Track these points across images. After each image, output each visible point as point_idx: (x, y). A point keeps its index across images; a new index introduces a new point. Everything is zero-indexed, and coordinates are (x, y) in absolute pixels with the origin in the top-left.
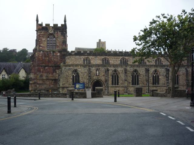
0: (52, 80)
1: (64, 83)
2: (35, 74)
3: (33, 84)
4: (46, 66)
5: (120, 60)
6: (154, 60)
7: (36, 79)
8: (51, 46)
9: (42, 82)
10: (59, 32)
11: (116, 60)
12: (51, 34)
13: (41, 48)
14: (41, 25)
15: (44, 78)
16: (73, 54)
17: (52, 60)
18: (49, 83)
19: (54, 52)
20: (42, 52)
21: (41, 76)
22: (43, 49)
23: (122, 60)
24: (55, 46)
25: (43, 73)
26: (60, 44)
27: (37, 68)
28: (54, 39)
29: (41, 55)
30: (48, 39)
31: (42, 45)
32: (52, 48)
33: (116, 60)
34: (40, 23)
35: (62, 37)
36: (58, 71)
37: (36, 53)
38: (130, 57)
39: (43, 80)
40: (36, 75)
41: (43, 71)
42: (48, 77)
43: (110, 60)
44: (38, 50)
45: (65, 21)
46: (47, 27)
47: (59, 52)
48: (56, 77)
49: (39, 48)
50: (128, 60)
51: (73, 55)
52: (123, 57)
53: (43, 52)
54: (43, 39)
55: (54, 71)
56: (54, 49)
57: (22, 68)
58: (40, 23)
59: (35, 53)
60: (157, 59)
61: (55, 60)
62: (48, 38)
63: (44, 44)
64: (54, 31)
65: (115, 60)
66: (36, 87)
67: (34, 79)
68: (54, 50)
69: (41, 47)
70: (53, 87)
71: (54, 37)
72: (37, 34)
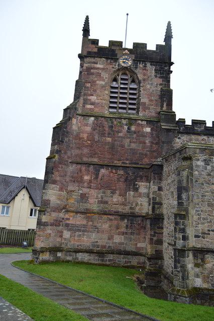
0: (123, 216)
1: (200, 227)
2: (61, 189)
3: (52, 225)
4: (102, 166)
7: (65, 209)
8: (120, 106)
9: (84, 222)
10: (148, 65)
12: (124, 70)
13: (89, 106)
14: (95, 42)
15: (95, 207)
16: (199, 130)
17: (123, 146)
18: (110, 226)
19: (131, 121)
20: (92, 119)
21: (84, 197)
22: (96, 110)
24: (135, 107)
25: (90, 187)
26: (151, 100)
27: (72, 168)
28: (131, 87)
29: (89, 129)
30: (114, 84)
31: (93, 98)
32: (125, 111)
34: (92, 36)
35: (160, 81)
36: (143, 187)
37: (74, 121)
39: (86, 213)
40: (64, 193)
41: (90, 181)
42: (106, 202)
44: (80, 111)
45: (168, 37)
46: (113, 48)
47: (149, 122)
48: (137, 204)
49: (84, 106)
51: (199, 134)
53: (96, 117)
54: (98, 82)
55: (131, 184)
56: (133, 114)
57: (24, 187)
58: (92, 36)
59: (70, 119)
61: (133, 146)
62: (114, 83)
63: (100, 100)
64: (136, 61)
66: (59, 239)
67: (58, 209)
68: (131, 116)
69: (92, 104)
70: (121, 244)
71: (133, 81)
72: (82, 66)
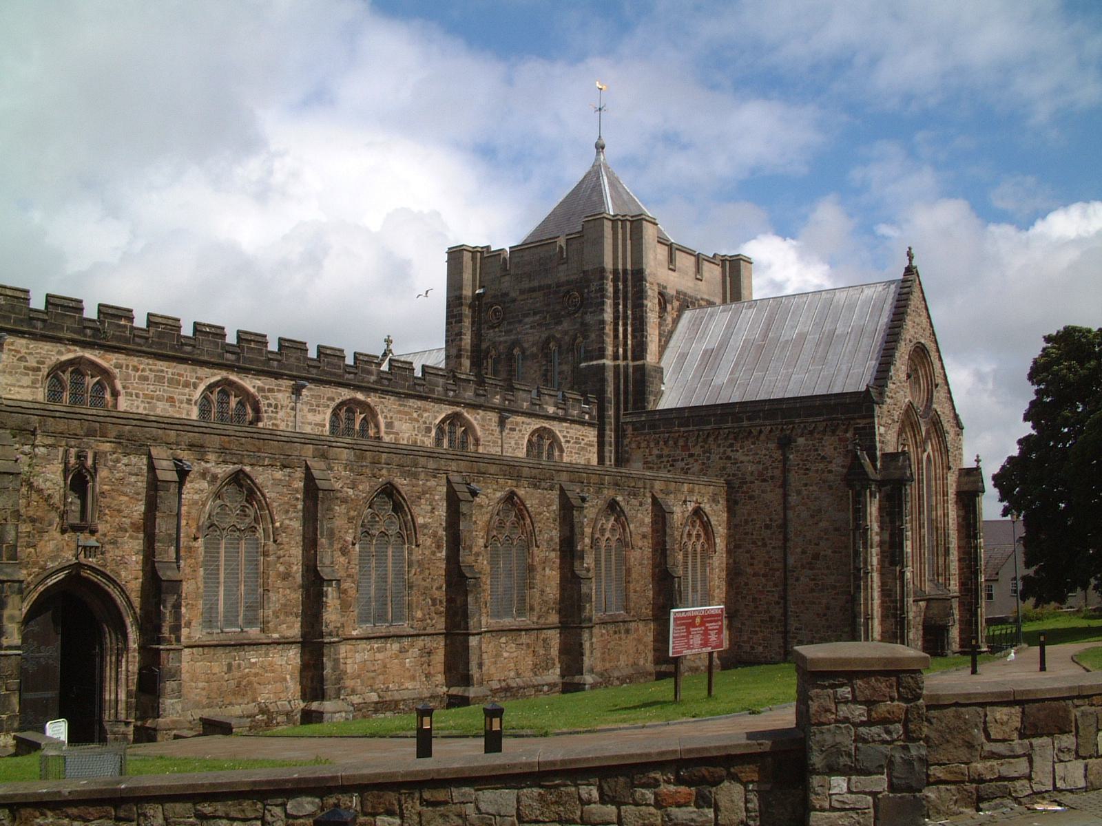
5: (197, 395)
6: (428, 430)
11: (171, 400)
23: (214, 397)
33: (171, 400)
38: (270, 383)
43: (119, 386)
50: (257, 410)
52: (224, 374)
60: (443, 421)
65: (164, 390)
